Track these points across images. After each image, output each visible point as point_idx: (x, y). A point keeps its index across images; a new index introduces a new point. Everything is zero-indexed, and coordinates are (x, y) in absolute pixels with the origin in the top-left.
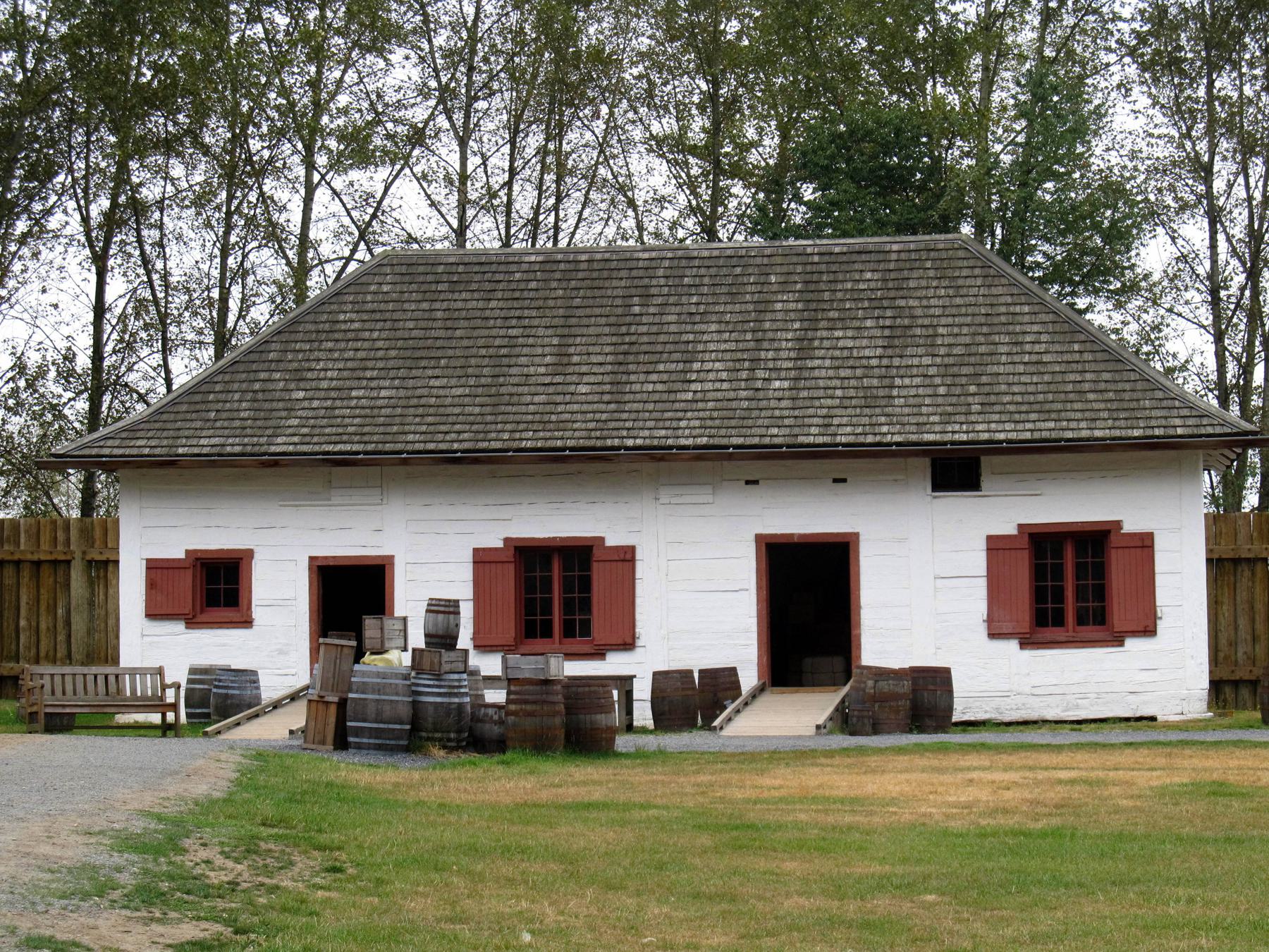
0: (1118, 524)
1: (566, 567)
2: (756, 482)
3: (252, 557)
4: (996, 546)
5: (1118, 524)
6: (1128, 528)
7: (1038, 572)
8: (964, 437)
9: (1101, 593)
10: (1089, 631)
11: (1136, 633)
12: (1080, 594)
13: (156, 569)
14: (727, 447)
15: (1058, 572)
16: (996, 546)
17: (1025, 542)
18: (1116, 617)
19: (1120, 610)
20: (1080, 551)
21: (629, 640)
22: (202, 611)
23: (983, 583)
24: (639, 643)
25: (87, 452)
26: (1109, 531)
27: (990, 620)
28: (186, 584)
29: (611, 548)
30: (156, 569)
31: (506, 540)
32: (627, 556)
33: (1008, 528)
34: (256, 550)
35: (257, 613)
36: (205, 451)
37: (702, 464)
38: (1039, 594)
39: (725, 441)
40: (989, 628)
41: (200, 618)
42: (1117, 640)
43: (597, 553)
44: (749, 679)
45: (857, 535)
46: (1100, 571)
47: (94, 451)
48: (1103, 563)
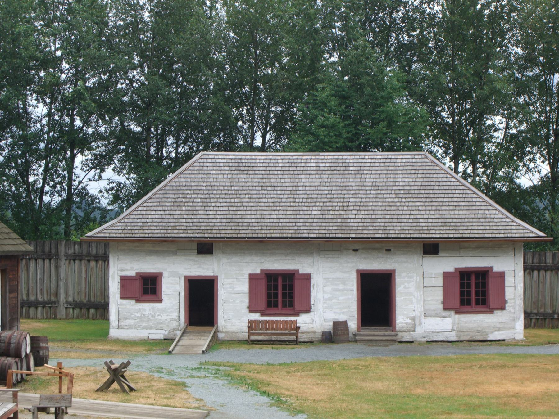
0: (491, 268)
1: (284, 281)
2: (389, 250)
3: (162, 275)
4: (446, 276)
5: (491, 268)
6: (495, 269)
7: (269, 287)
8: (438, 236)
9: (291, 296)
10: (480, 308)
11: (498, 309)
12: (477, 294)
13: (125, 281)
14: (349, 238)
15: (469, 285)
16: (253, 278)
17: (458, 275)
18: (491, 303)
19: (492, 299)
20: (477, 278)
21: (308, 309)
22: (142, 296)
23: (442, 289)
24: (311, 310)
25: (99, 235)
26: (294, 274)
27: (444, 303)
28: (137, 286)
29: (302, 274)
30: (125, 281)
31: (456, 269)
32: (307, 278)
33: (451, 269)
34: (163, 273)
35: (164, 297)
36: (147, 235)
37: (165, 243)
38: (269, 296)
39: (348, 236)
40: (444, 306)
41: (141, 299)
42: (491, 311)
43: (296, 276)
44: (353, 325)
45: (394, 271)
46: (291, 287)
47: (102, 235)
48: (292, 284)
